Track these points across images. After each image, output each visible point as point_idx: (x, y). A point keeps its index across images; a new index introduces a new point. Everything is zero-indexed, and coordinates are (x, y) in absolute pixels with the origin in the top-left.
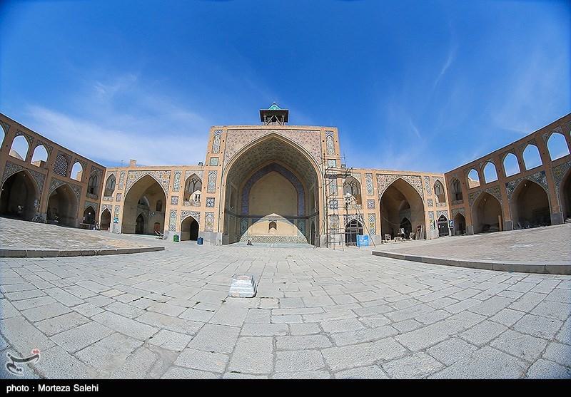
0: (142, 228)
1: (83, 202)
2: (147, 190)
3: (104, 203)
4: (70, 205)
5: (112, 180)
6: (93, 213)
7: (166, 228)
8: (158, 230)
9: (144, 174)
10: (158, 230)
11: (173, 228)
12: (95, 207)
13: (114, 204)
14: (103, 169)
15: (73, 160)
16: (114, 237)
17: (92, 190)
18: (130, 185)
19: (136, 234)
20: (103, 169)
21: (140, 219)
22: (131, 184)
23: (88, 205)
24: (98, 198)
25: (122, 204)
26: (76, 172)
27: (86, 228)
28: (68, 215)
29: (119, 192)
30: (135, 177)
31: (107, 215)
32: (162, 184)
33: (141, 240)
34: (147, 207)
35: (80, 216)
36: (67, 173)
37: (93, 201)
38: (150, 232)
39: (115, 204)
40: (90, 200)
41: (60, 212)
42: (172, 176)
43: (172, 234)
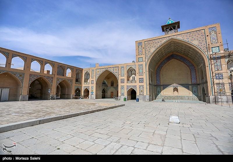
0: (104, 95)
1: (74, 87)
2: (106, 77)
3: (84, 86)
4: (67, 89)
5: (87, 74)
6: (80, 91)
7: (119, 94)
8: (115, 95)
9: (104, 70)
10: (115, 95)
11: (123, 94)
12: (79, 88)
13: (90, 85)
14: (81, 70)
15: (66, 68)
16: (93, 102)
17: (78, 80)
18: (98, 76)
19: (102, 98)
20: (81, 70)
21: (103, 91)
22: (98, 75)
23: (76, 88)
24: (81, 83)
25: (94, 85)
26: (69, 73)
27: (76, 98)
28: (66, 93)
29: (92, 79)
30: (101, 72)
31: (87, 92)
32: (115, 74)
33: (108, 101)
34: (108, 85)
35: (73, 93)
36: (63, 74)
37: (79, 85)
38: (108, 97)
39: (91, 85)
40: (77, 85)
41: (63, 92)
42: (120, 70)
43: (123, 97)
